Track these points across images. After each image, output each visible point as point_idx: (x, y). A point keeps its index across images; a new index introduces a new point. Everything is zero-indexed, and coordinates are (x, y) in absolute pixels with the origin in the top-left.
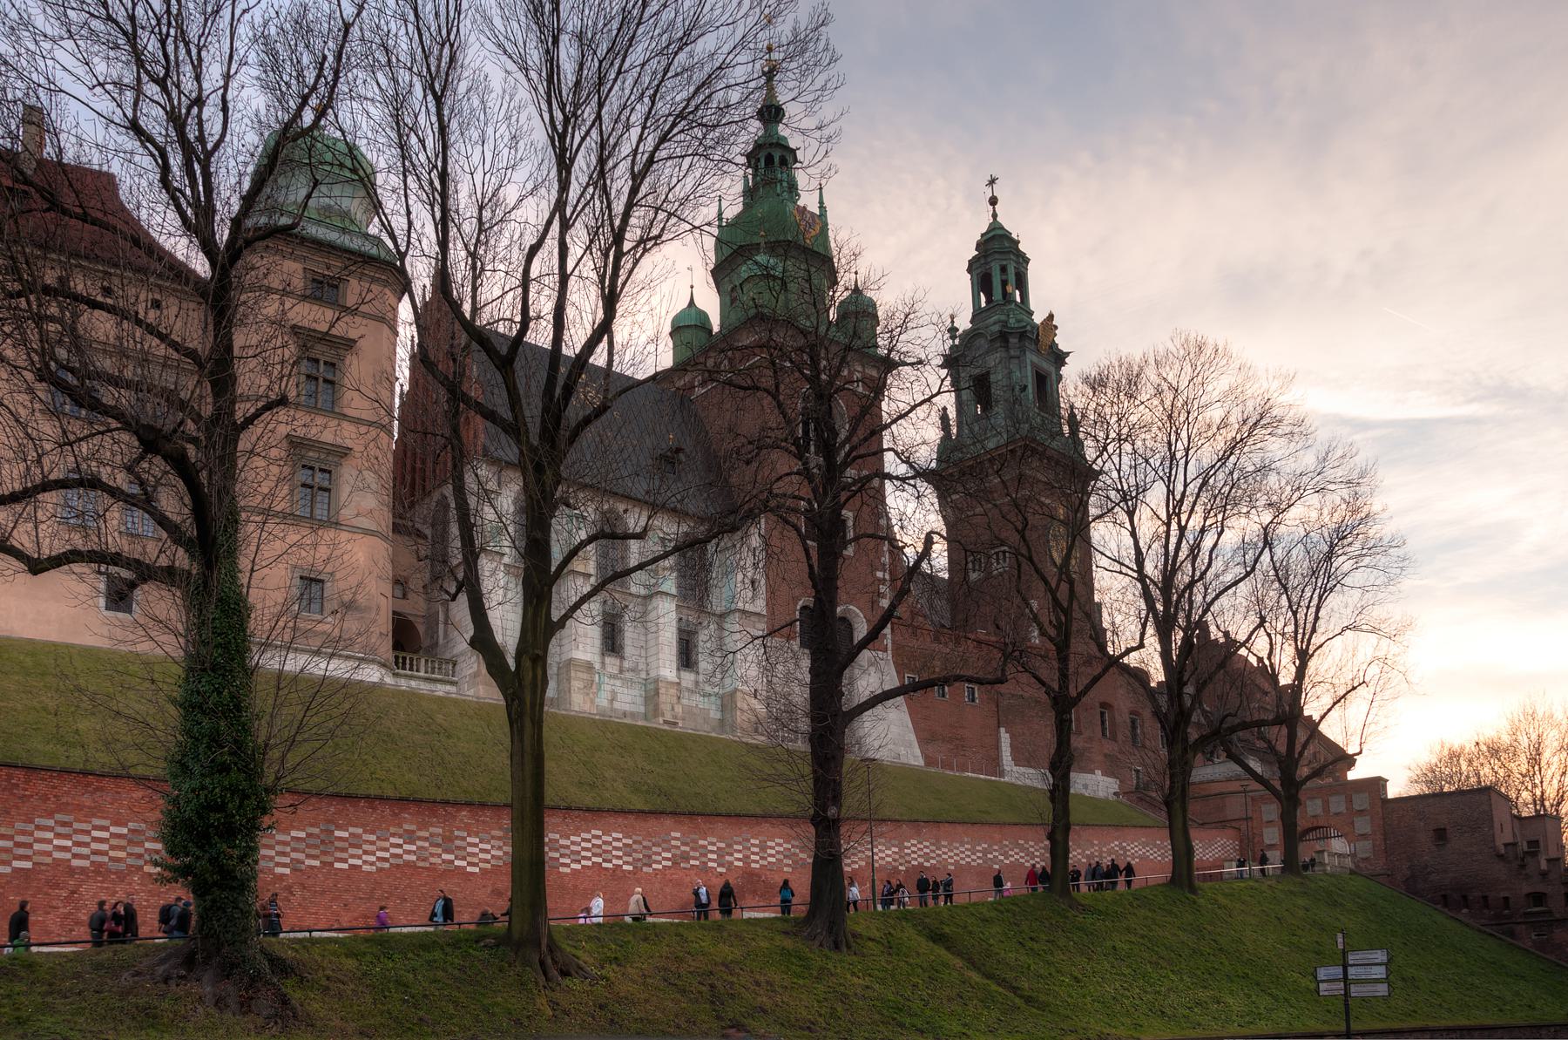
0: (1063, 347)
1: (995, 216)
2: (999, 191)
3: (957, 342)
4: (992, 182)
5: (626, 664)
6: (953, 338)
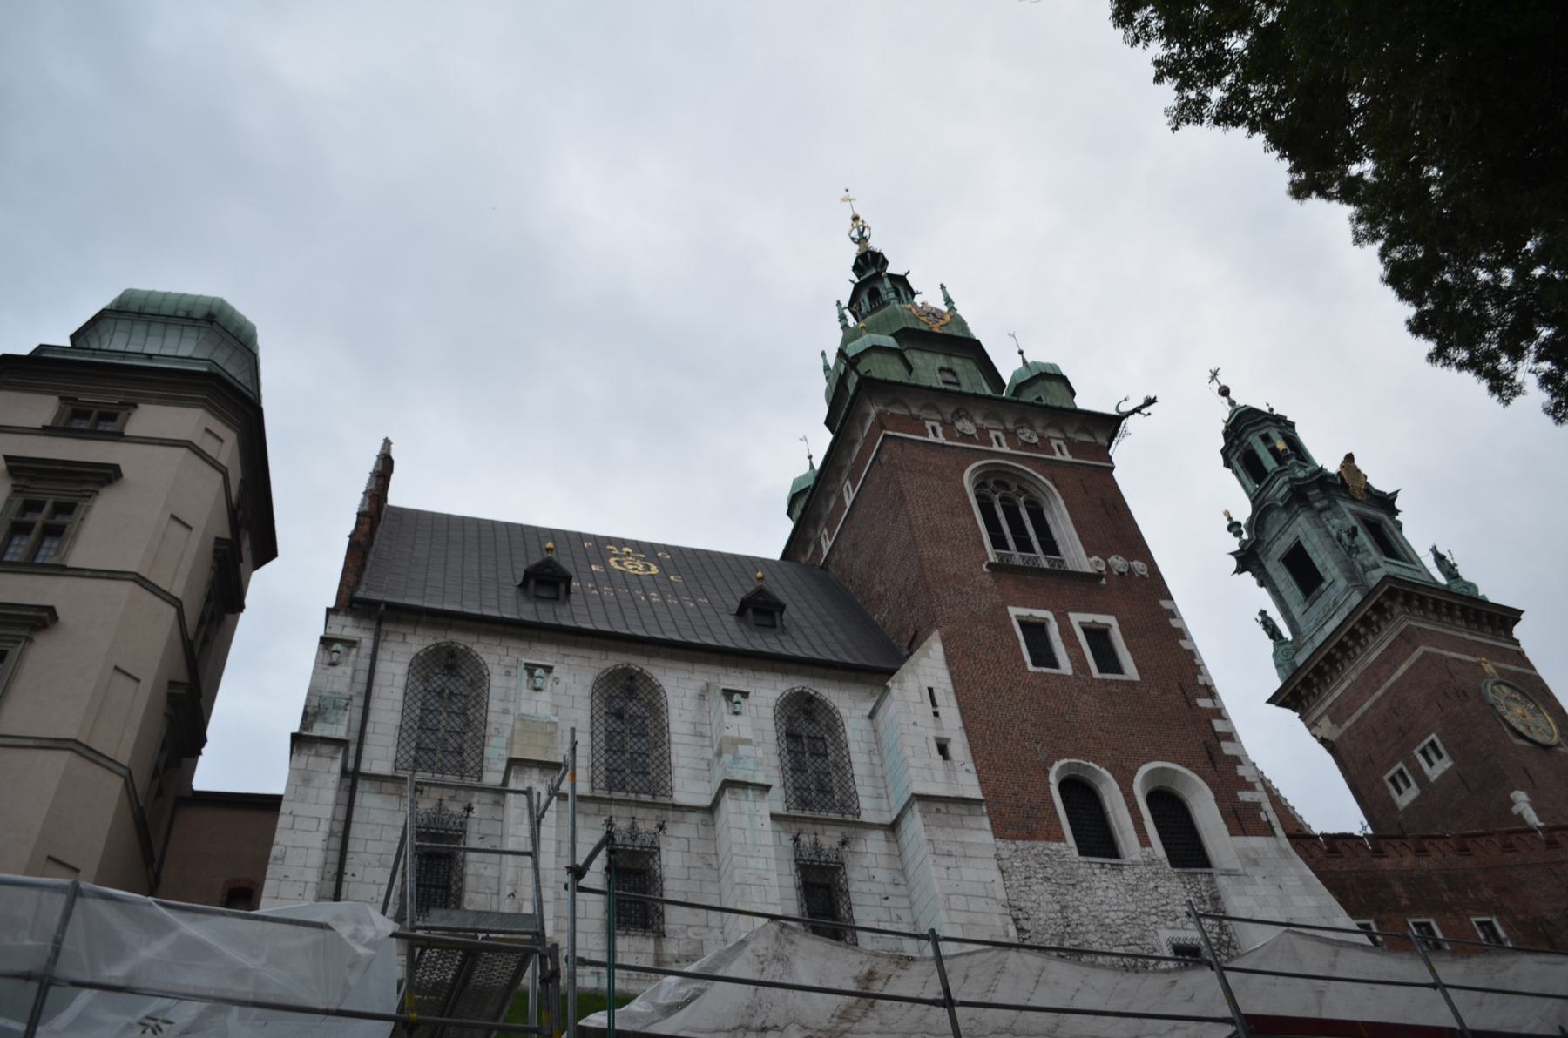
1: (1232, 403)
2: (1224, 380)
3: (1245, 536)
4: (1214, 375)
6: (1238, 534)
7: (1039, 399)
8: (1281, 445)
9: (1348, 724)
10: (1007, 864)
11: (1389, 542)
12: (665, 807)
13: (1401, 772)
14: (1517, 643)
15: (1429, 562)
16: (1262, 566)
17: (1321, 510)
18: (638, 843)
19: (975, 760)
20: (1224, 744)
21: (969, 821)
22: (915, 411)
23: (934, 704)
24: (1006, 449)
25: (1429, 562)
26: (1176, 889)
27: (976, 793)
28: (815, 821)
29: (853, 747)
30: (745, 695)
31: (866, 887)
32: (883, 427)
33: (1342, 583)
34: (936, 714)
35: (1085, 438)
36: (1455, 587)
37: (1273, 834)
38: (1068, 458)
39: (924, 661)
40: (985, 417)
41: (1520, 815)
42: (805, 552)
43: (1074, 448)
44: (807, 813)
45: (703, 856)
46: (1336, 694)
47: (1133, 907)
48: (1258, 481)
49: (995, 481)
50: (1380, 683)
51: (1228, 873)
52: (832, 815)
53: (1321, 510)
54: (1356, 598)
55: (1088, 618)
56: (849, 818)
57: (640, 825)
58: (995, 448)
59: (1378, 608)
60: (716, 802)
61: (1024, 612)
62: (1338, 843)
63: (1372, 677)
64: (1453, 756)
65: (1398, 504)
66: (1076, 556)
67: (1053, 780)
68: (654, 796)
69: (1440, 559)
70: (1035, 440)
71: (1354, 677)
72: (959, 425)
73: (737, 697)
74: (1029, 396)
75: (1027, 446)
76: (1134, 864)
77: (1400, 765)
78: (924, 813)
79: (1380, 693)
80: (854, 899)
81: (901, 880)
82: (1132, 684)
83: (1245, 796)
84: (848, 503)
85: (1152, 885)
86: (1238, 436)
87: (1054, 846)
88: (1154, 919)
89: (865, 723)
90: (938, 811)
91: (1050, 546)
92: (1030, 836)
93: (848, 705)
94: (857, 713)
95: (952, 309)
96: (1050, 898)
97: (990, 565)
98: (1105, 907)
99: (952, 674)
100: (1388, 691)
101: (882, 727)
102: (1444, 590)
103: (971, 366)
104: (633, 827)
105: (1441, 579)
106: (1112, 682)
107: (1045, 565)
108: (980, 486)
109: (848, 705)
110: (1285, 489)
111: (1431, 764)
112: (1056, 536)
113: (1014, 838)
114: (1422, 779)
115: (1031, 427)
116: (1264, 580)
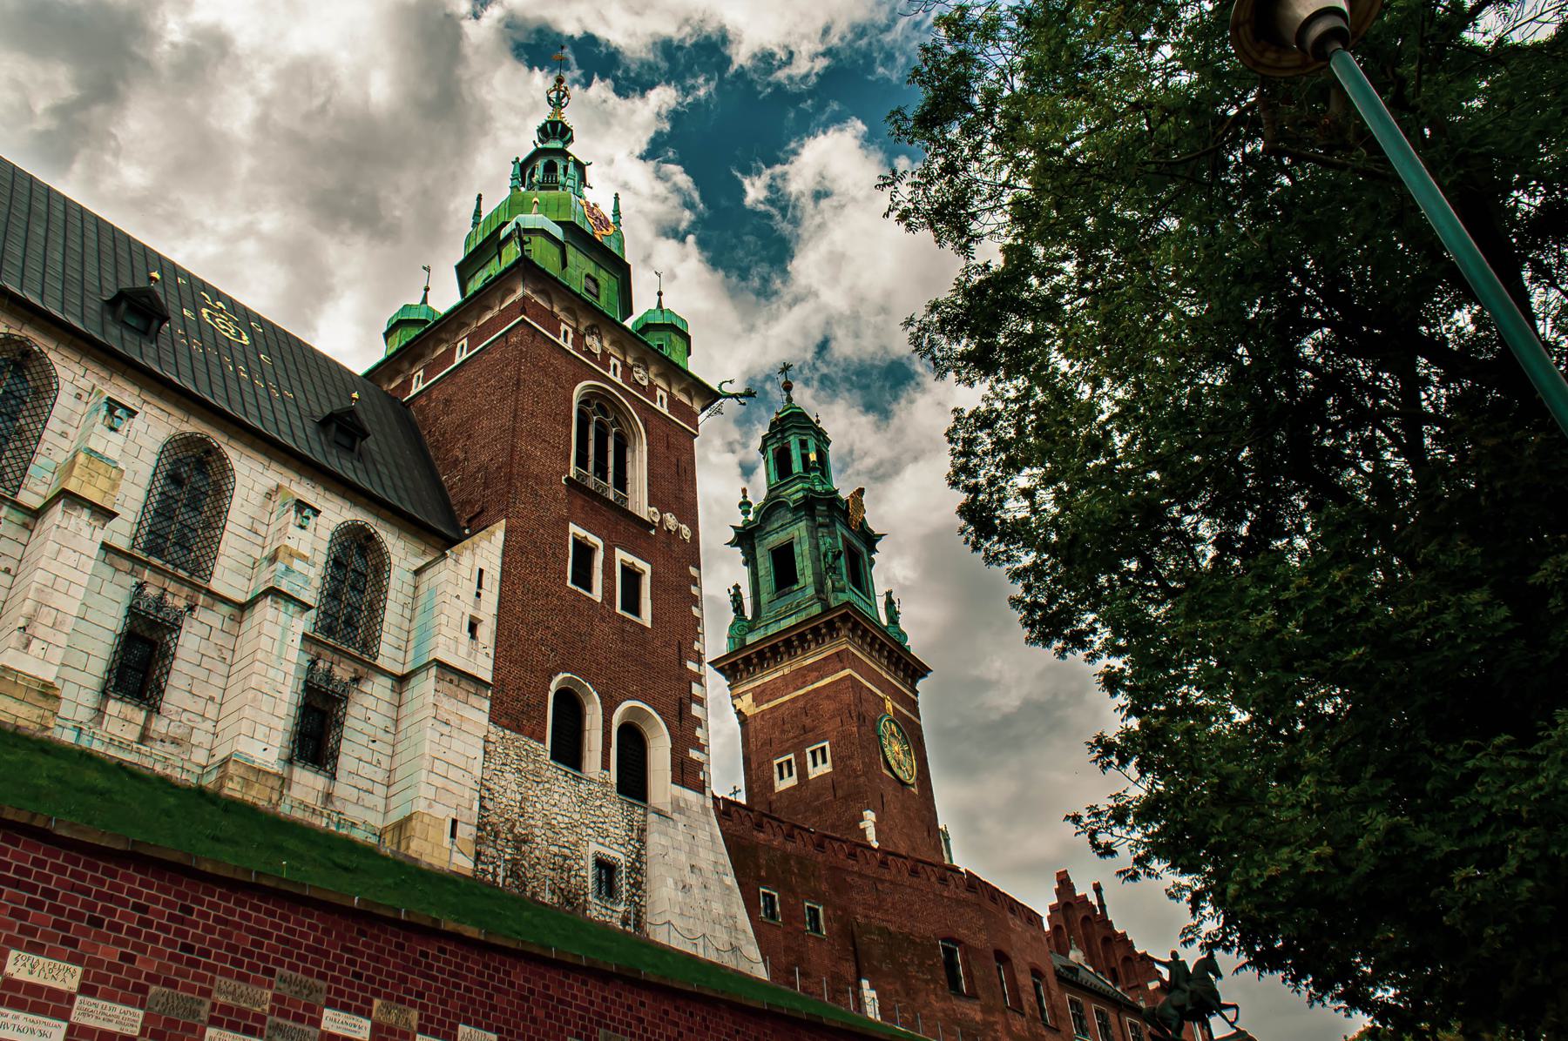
0: (874, 526)
3: (751, 517)
5: (160, 726)
6: (746, 513)
7: (661, 346)
8: (813, 457)
9: (765, 707)
10: (491, 747)
11: (859, 578)
12: (198, 588)
13: (789, 762)
14: (916, 693)
16: (754, 549)
17: (821, 525)
18: (161, 615)
19: (496, 647)
20: (694, 706)
21: (473, 699)
22: (556, 310)
23: (480, 586)
24: (618, 380)
25: (881, 603)
26: (614, 810)
27: (488, 677)
28: (335, 650)
29: (391, 595)
30: (317, 512)
31: (360, 725)
32: (523, 312)
33: (810, 591)
34: (478, 595)
35: (685, 400)
37: (703, 792)
38: (665, 411)
39: (484, 544)
40: (612, 343)
41: (864, 830)
42: (391, 380)
43: (674, 404)
44: (331, 641)
45: (220, 648)
46: (767, 679)
47: (577, 816)
48: (781, 478)
49: (599, 401)
50: (804, 684)
51: (659, 813)
52: (351, 650)
53: (821, 525)
54: (816, 609)
55: (630, 558)
56: (366, 657)
57: (169, 597)
58: (610, 375)
59: (830, 626)
60: (253, 603)
61: (582, 533)
62: (733, 809)
63: (802, 677)
64: (834, 766)
65: (878, 546)
66: (639, 502)
67: (553, 687)
68: (192, 574)
69: (890, 603)
70: (645, 383)
71: (786, 671)
72: (588, 340)
73: (307, 512)
74: (653, 340)
75: (636, 385)
76: (591, 781)
77: (791, 756)
78: (438, 679)
79: (801, 692)
80: (346, 733)
81: (392, 730)
82: (643, 628)
83: (694, 754)
84: (458, 361)
85: (598, 803)
86: (783, 431)
87: (534, 744)
88: (590, 831)
89: (409, 577)
90: (451, 681)
91: (621, 482)
92: (519, 729)
93: (400, 552)
94: (406, 565)
95: (618, 223)
96: (515, 788)
97: (569, 479)
98: (556, 810)
99: (503, 563)
100: (808, 693)
101: (423, 588)
102: (883, 630)
103: (614, 284)
104: (161, 597)
105: (884, 621)
106: (630, 621)
107: (611, 497)
108: (584, 402)
110: (801, 494)
111: (815, 764)
112: (629, 475)
113: (505, 727)
114: (803, 774)
115: (647, 369)
116: (751, 560)
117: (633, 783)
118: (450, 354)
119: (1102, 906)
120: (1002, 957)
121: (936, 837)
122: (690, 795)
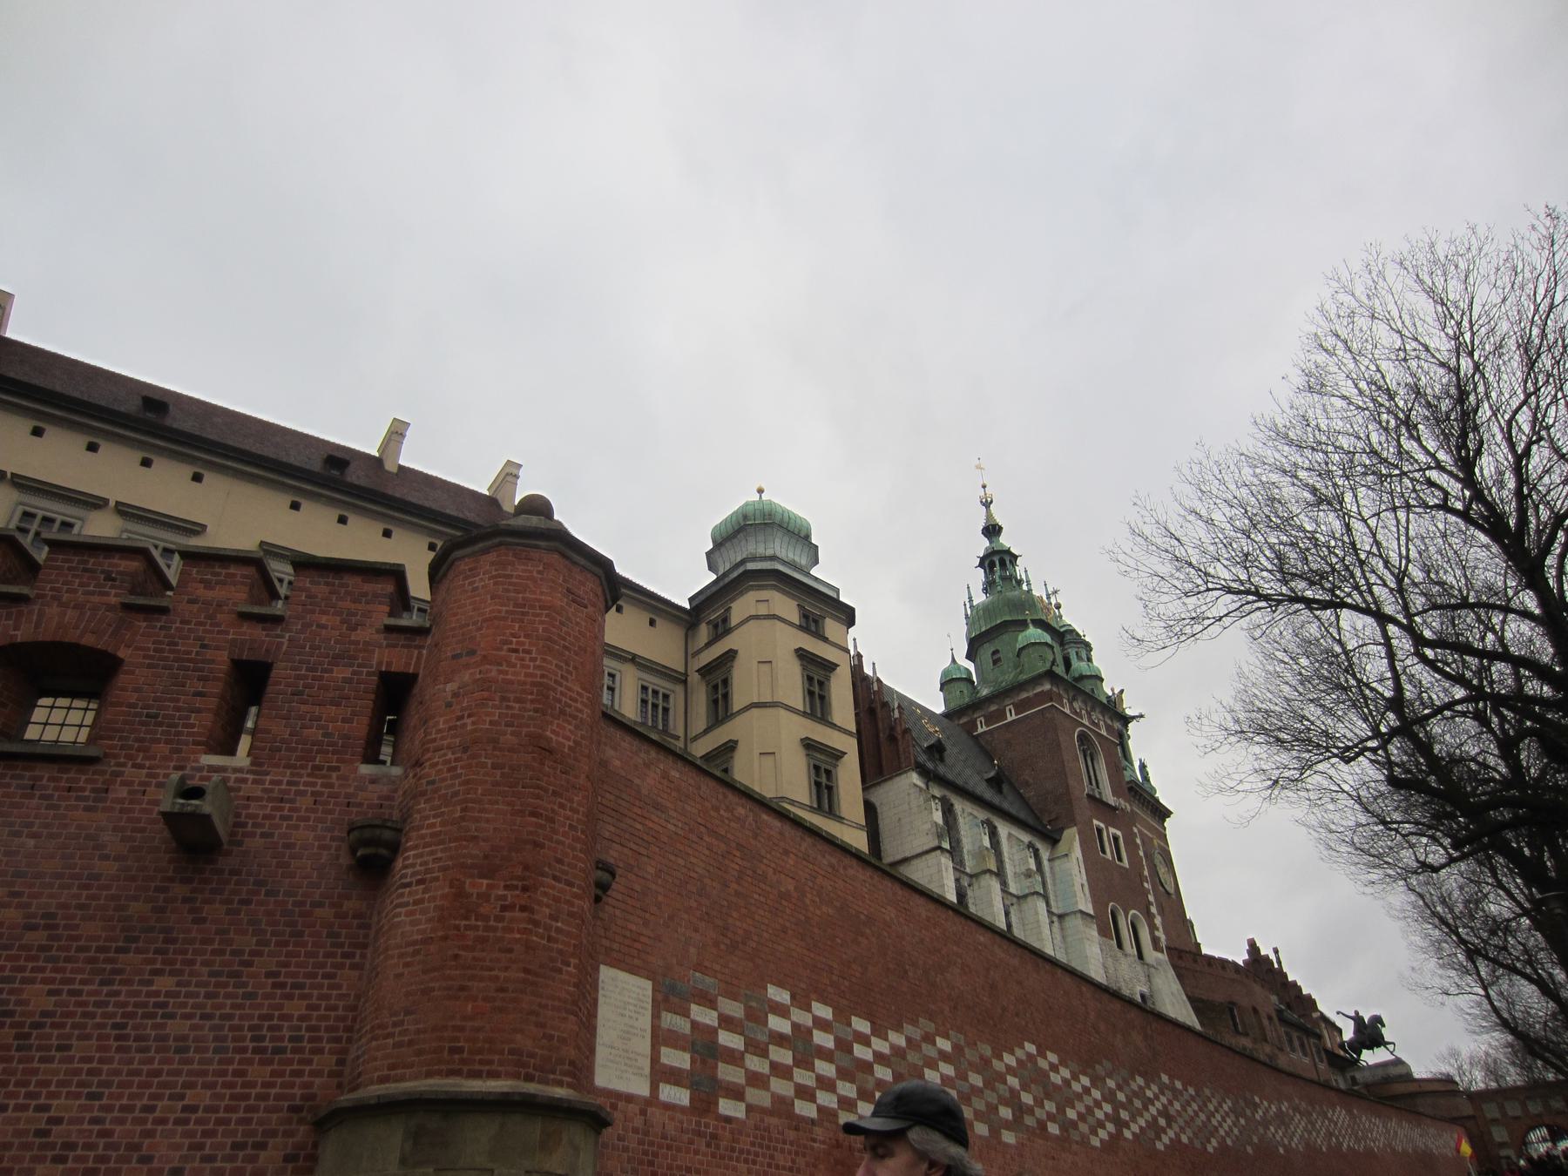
15: (1137, 765)
25: (1137, 765)
36: (1146, 786)
49: (1083, 738)
60: (1025, 897)
74: (1087, 686)
75: (1093, 723)
84: (1009, 719)
101: (1057, 869)
109: (1045, 855)
117: (1140, 956)
118: (1001, 714)
119: (1279, 962)
120: (1255, 1010)
121: (1187, 926)
122: (1159, 955)
